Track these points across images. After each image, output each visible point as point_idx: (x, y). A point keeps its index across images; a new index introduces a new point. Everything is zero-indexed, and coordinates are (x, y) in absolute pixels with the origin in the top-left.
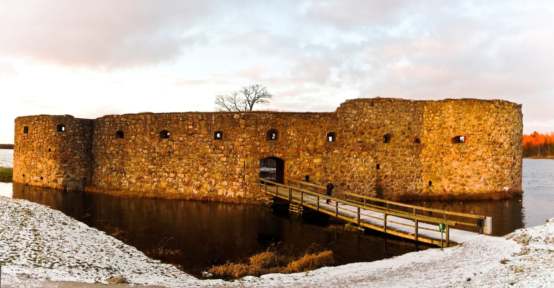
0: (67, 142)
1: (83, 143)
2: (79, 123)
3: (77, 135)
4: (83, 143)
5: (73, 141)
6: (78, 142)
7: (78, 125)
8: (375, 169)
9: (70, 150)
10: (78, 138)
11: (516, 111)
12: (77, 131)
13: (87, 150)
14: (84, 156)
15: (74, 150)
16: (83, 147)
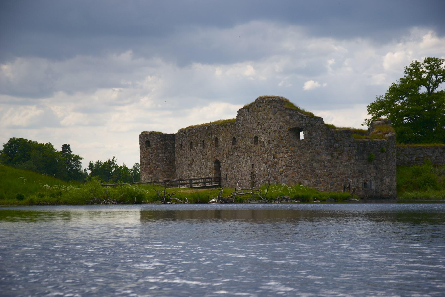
0: (152, 156)
1: (165, 156)
2: (160, 139)
3: (159, 149)
4: (165, 156)
5: (156, 154)
6: (160, 155)
7: (159, 140)
8: (251, 168)
9: (154, 162)
10: (160, 151)
11: (269, 106)
12: (158, 145)
13: (170, 162)
14: (166, 167)
15: (158, 162)
16: (165, 160)
